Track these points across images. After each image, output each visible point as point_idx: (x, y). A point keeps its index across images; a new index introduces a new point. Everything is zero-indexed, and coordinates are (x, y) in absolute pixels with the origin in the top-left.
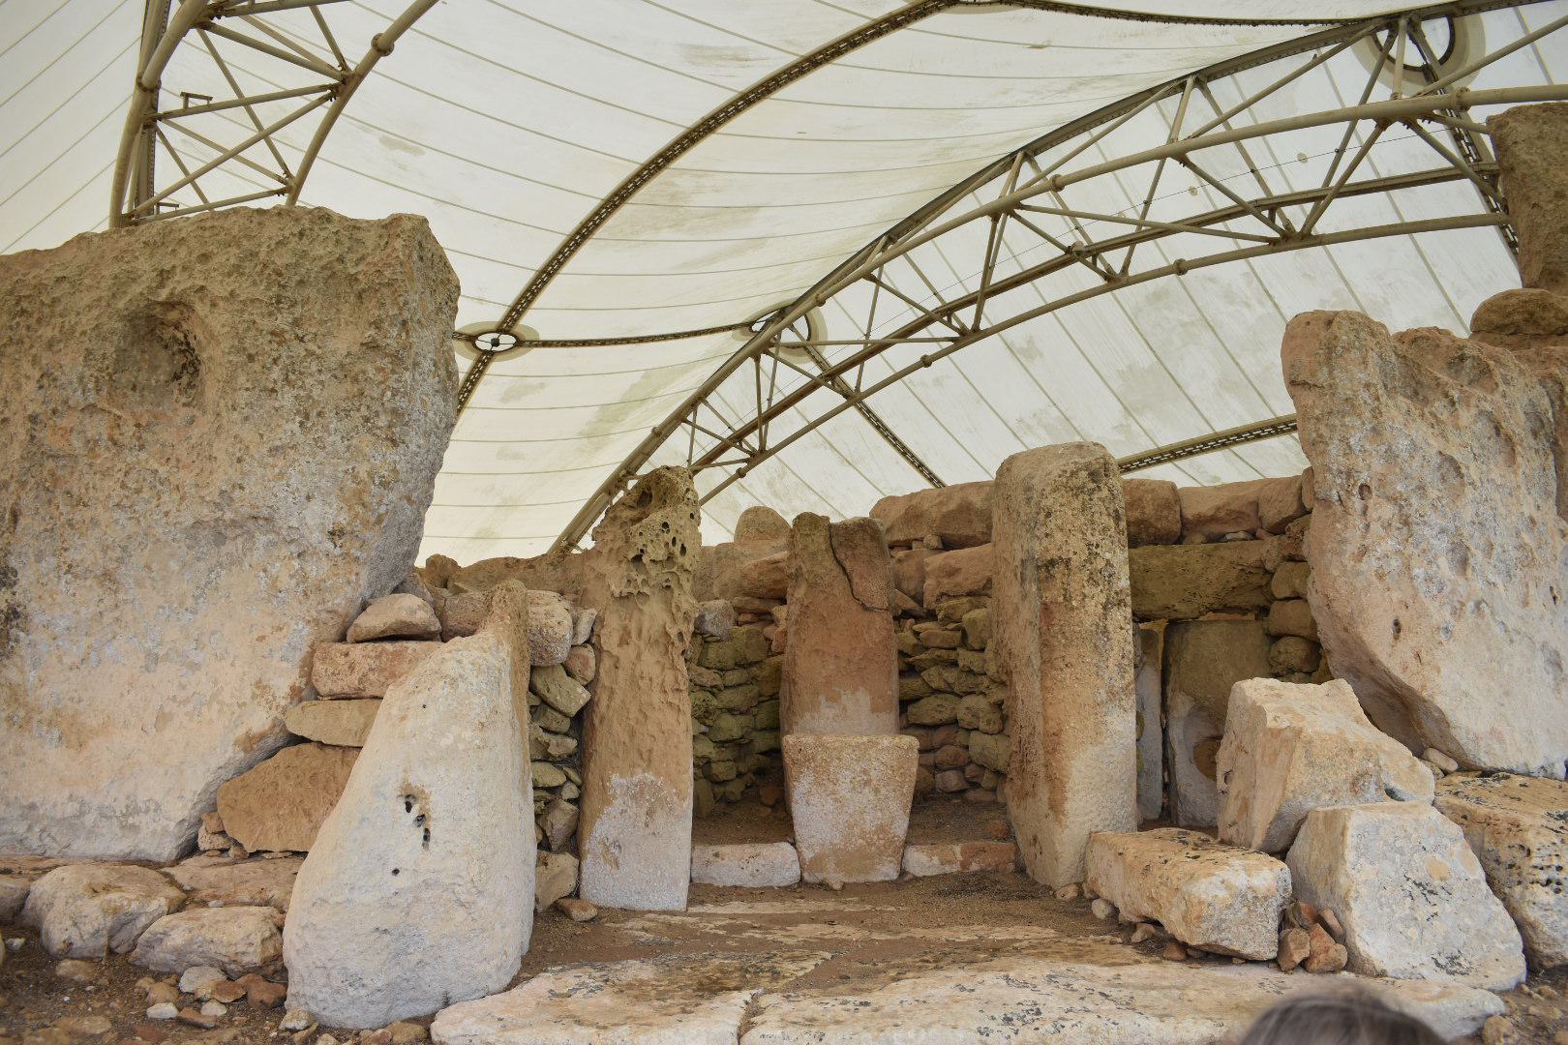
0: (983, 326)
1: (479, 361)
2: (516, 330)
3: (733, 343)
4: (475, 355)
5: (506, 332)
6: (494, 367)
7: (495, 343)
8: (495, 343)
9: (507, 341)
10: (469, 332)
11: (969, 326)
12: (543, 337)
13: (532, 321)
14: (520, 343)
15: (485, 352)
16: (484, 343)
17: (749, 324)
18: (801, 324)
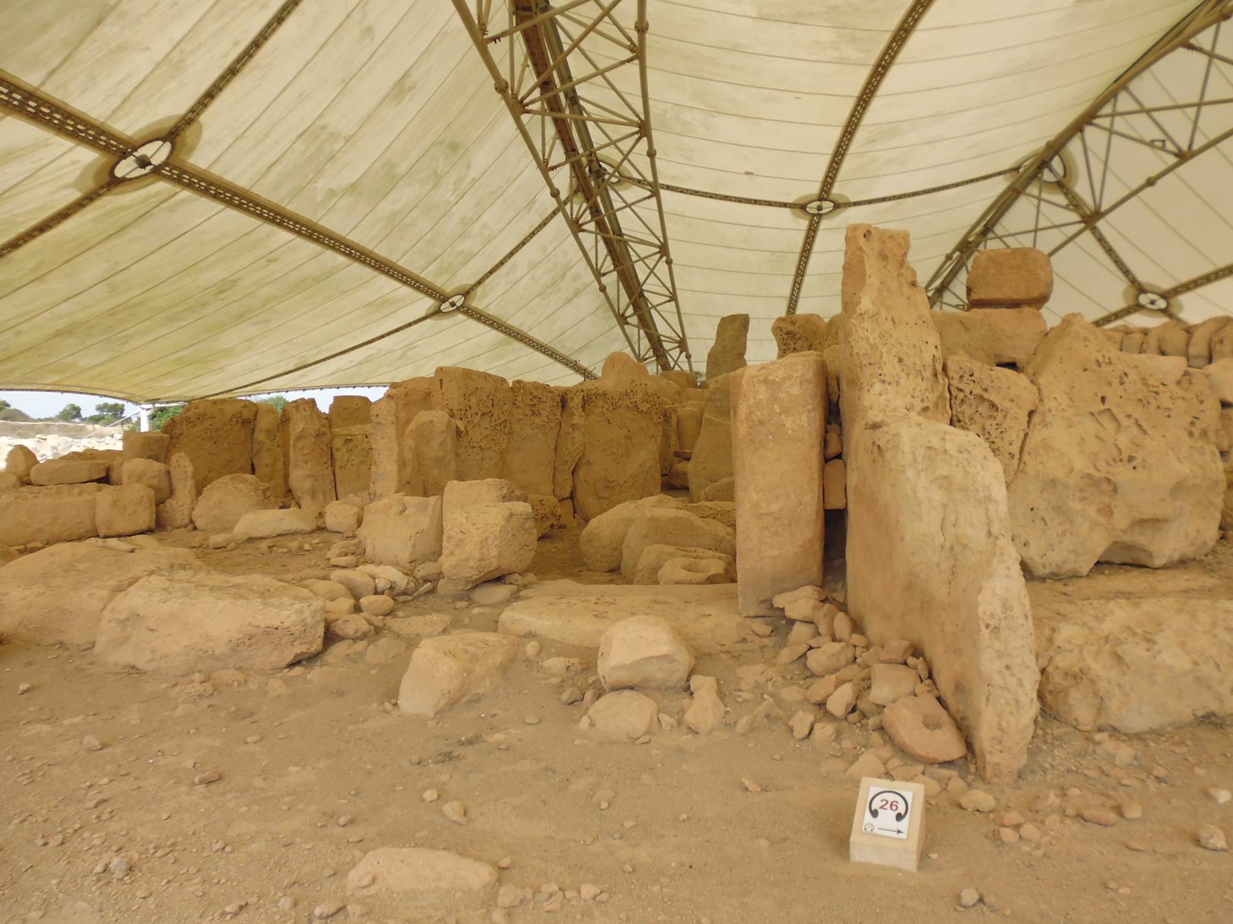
0: (1196, 147)
1: (812, 220)
2: (831, 197)
3: (1000, 186)
4: (809, 217)
5: (825, 200)
6: (824, 224)
7: (820, 208)
8: (820, 208)
9: (827, 206)
10: (802, 202)
11: (1185, 147)
12: (852, 200)
13: (836, 190)
14: (837, 206)
15: (814, 215)
16: (812, 208)
17: (1017, 169)
18: (1056, 163)
